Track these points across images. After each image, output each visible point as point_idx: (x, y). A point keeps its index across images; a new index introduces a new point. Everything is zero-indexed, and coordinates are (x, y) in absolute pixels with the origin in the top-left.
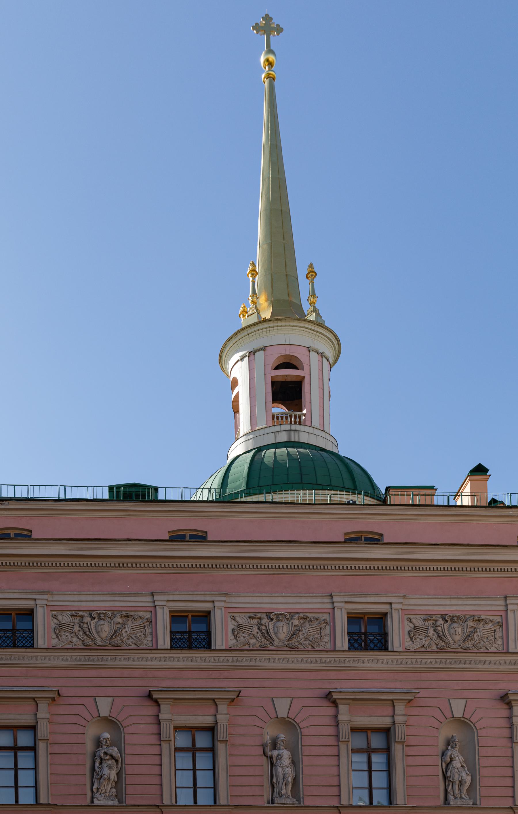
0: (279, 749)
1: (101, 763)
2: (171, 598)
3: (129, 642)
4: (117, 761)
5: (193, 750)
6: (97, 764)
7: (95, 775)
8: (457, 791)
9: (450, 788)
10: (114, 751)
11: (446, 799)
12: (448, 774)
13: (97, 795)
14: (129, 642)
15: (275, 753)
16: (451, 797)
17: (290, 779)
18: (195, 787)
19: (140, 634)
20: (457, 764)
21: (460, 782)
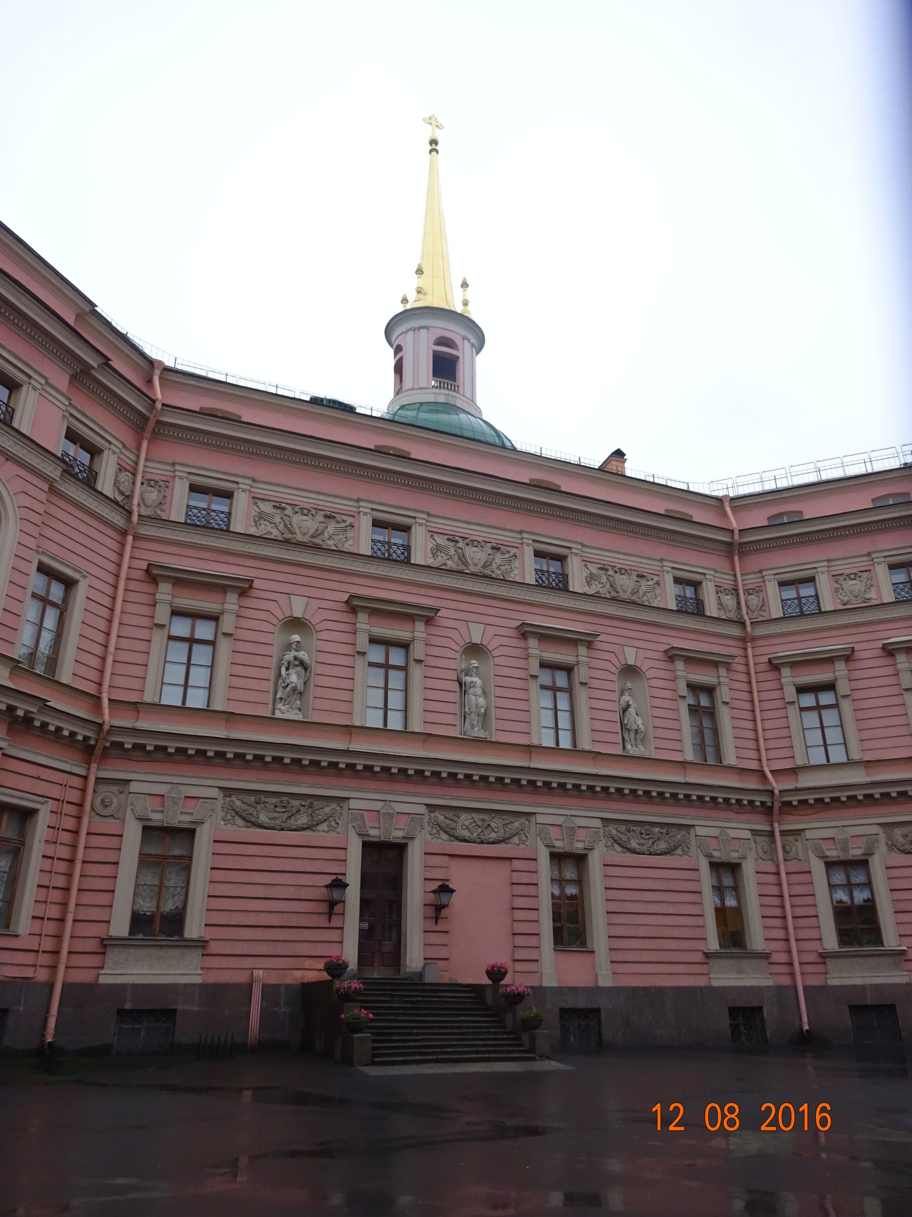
0: (471, 676)
1: (287, 669)
2: (375, 507)
3: (331, 542)
4: (306, 669)
5: (387, 667)
6: (283, 670)
7: (280, 681)
8: (633, 740)
9: (626, 736)
10: (302, 655)
11: (624, 748)
12: (626, 722)
13: (279, 706)
14: (331, 542)
15: (468, 679)
16: (629, 746)
17: (483, 710)
18: (386, 708)
19: (341, 536)
20: (632, 710)
21: (636, 730)
